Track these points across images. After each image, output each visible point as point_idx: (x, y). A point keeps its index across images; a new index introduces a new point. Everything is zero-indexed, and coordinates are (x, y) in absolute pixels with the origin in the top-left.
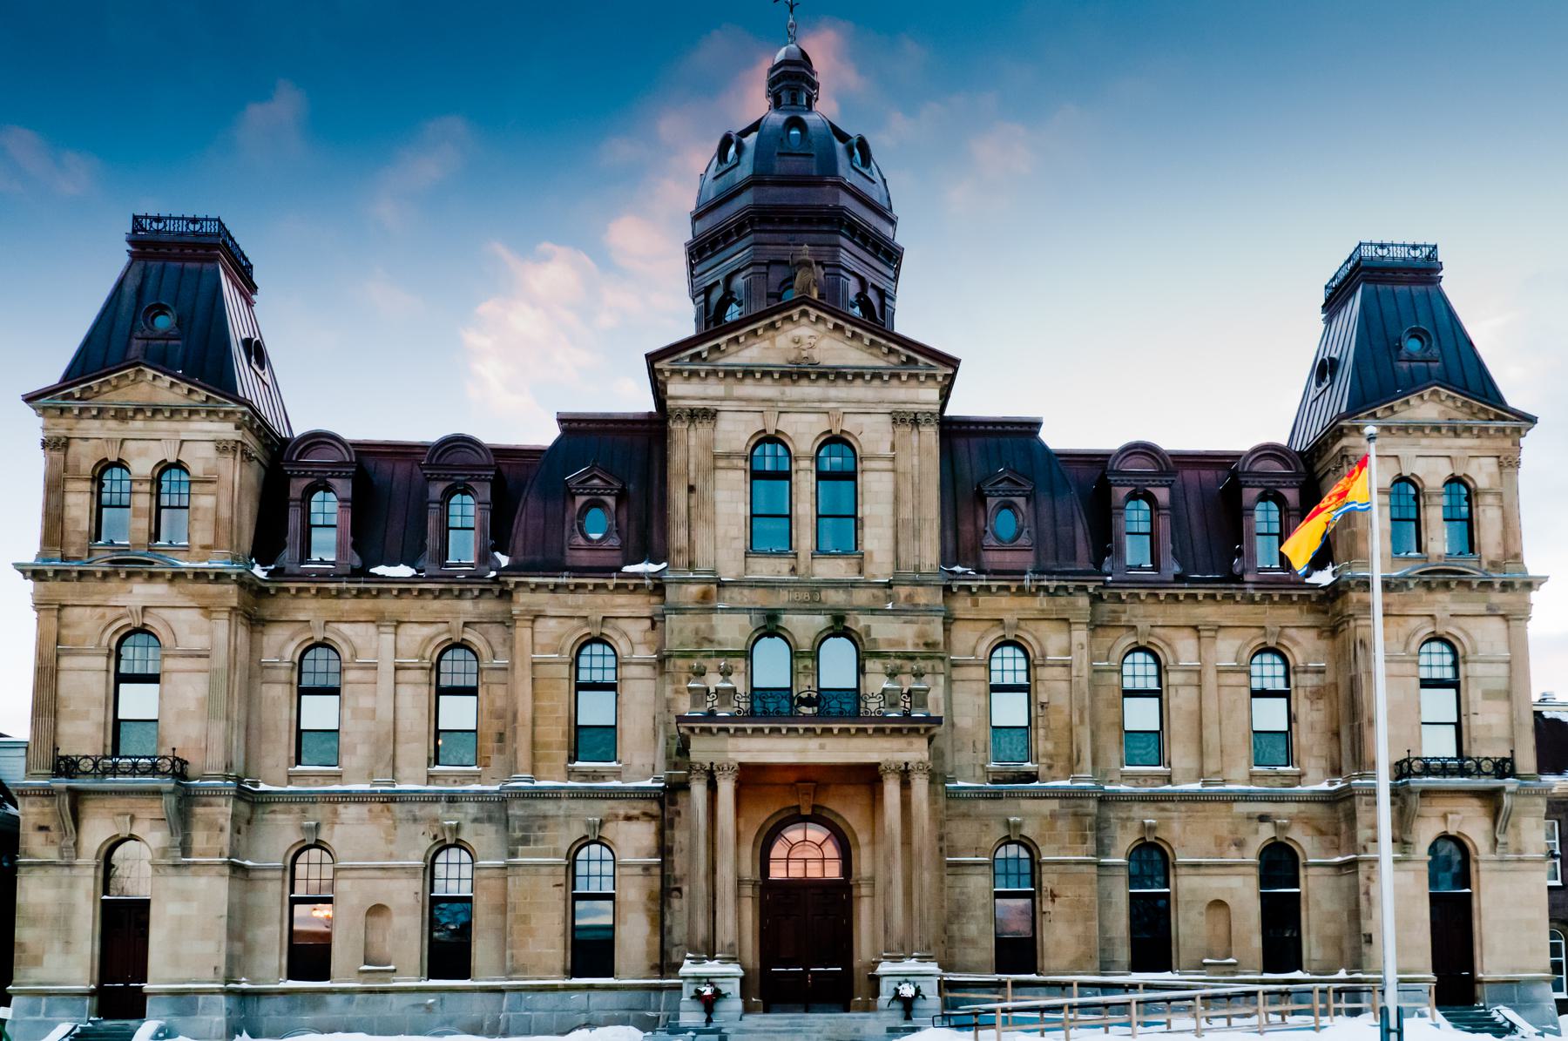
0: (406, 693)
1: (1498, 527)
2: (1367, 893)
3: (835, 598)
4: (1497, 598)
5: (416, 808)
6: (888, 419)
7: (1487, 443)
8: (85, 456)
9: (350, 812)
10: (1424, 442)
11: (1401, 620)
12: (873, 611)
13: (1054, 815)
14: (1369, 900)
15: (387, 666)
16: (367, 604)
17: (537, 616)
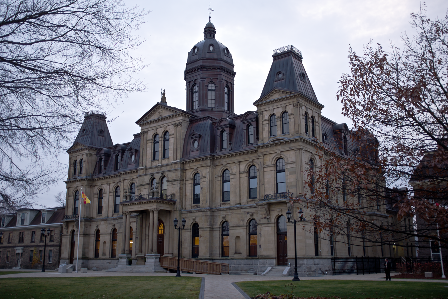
0: (110, 197)
1: (294, 124)
2: (260, 233)
3: (164, 169)
4: (292, 145)
5: (110, 221)
6: (173, 126)
7: (290, 101)
8: (74, 159)
9: (102, 222)
10: (275, 104)
11: (270, 155)
12: (168, 171)
13: (202, 216)
14: (260, 235)
15: (108, 193)
16: (106, 180)
17: (124, 180)
